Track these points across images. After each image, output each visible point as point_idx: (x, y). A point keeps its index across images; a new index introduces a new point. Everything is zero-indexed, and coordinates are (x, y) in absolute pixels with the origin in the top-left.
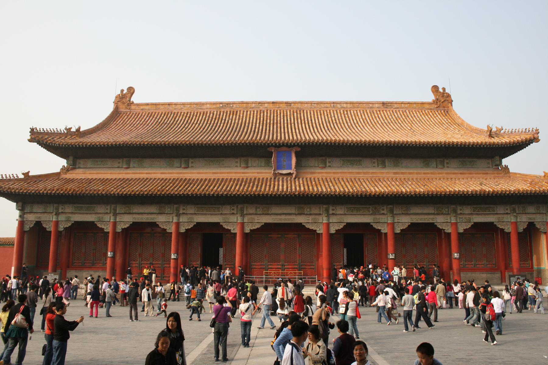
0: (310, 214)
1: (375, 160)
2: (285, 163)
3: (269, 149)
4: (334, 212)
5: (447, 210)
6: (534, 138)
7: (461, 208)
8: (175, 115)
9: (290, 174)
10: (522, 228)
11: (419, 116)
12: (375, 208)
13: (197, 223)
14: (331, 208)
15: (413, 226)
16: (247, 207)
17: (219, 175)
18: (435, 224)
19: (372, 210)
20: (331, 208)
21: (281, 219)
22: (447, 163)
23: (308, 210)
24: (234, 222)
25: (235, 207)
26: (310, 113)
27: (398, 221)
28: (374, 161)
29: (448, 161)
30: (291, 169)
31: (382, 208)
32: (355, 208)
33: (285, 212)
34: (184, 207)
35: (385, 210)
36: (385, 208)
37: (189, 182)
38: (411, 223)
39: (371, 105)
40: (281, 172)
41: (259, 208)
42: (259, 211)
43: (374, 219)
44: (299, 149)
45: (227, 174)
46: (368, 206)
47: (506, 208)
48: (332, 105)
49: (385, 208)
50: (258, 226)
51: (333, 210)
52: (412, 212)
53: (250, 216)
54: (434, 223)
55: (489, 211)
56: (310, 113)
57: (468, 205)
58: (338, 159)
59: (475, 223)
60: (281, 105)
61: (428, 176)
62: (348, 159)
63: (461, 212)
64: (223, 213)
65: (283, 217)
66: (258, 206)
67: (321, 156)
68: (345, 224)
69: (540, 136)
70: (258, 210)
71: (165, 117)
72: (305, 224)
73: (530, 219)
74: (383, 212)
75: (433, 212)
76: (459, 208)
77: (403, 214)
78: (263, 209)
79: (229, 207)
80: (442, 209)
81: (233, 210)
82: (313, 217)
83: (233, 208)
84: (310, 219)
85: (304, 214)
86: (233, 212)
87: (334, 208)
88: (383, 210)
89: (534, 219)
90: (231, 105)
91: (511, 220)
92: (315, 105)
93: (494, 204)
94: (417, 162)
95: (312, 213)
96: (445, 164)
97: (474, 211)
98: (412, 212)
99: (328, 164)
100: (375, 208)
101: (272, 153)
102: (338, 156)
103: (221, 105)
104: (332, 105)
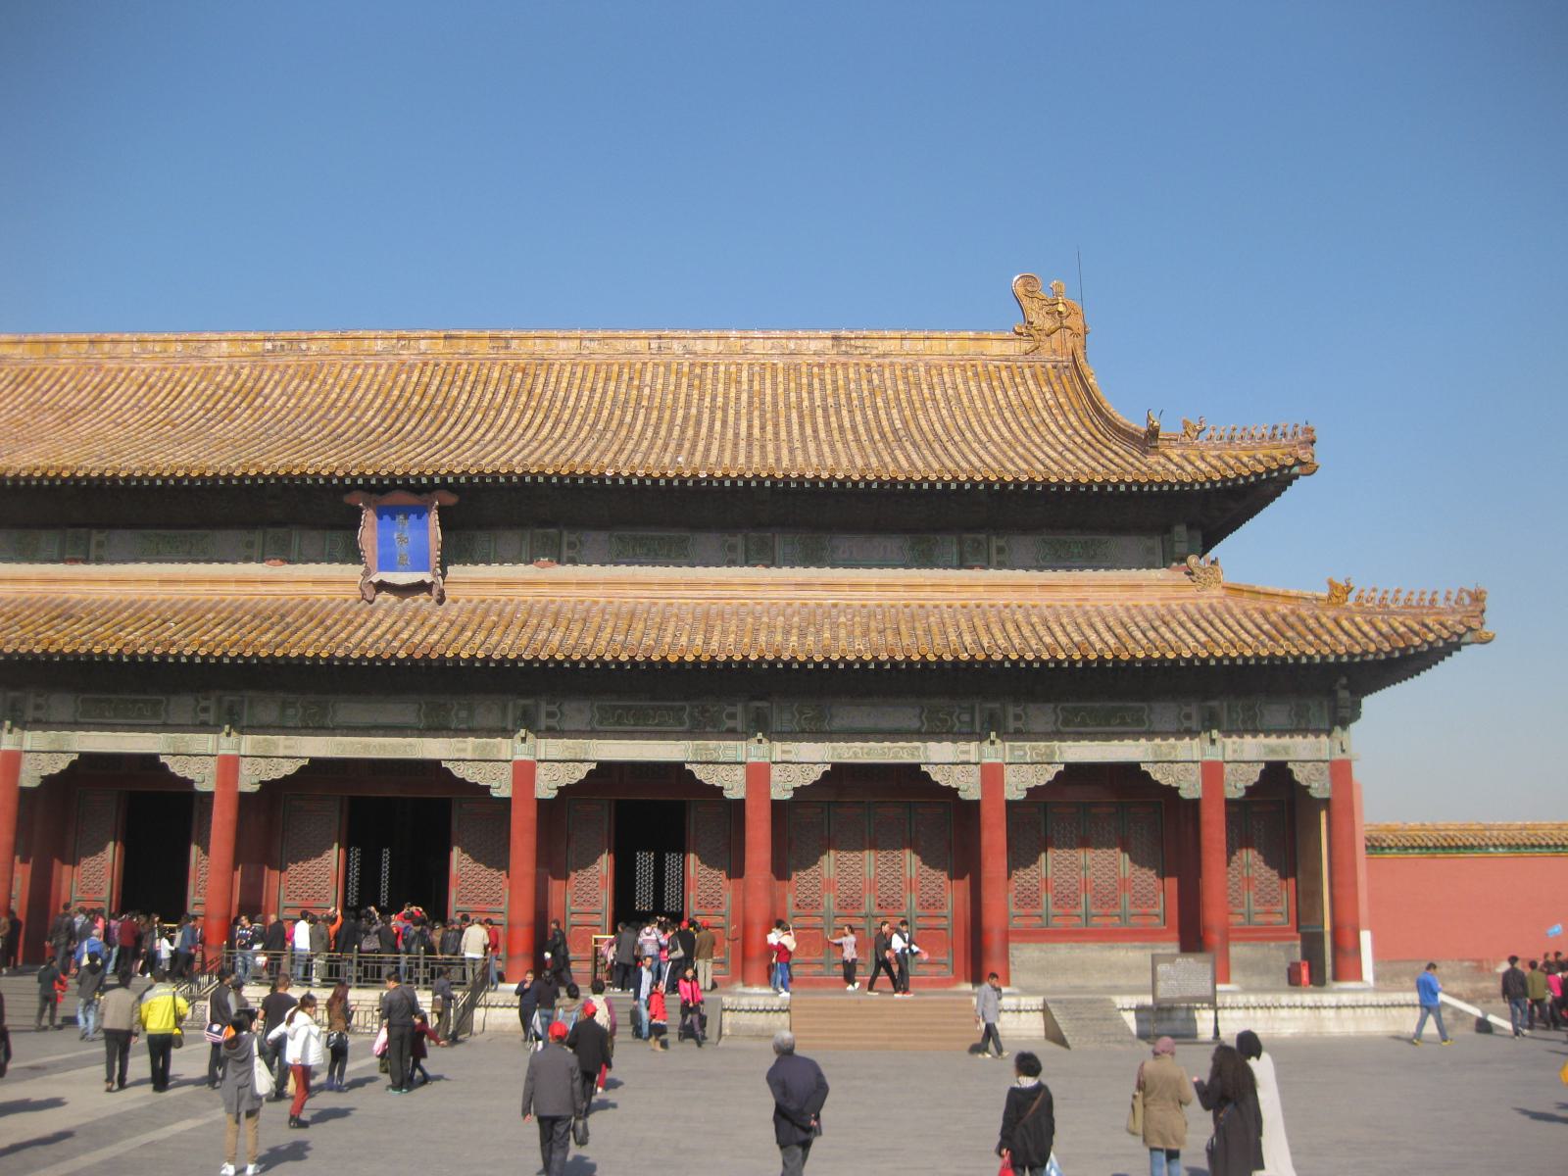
1: (739, 540)
2: (402, 549)
3: (347, 499)
4: (552, 722)
5: (966, 718)
6: (1299, 462)
7: (1018, 710)
8: (107, 380)
9: (422, 587)
10: (1241, 785)
11: (959, 381)
12: (704, 711)
13: (82, 755)
14: (544, 707)
15: (839, 774)
17: (181, 587)
18: (924, 768)
19: (691, 715)
20: (544, 707)
21: (367, 746)
22: (1000, 550)
23: (463, 714)
24: (208, 756)
25: (211, 703)
26: (573, 373)
27: (786, 758)
28: (732, 540)
29: (1002, 543)
30: (427, 570)
31: (730, 709)
32: (630, 708)
33: (383, 720)
34: (40, 701)
35: (739, 716)
36: (739, 709)
37: (65, 613)
38: (834, 765)
39: (792, 345)
40: (390, 577)
43: (697, 749)
44: (451, 500)
45: (207, 587)
46: (678, 704)
47: (1187, 710)
48: (654, 344)
49: (739, 709)
50: (289, 768)
51: (551, 715)
52: (837, 724)
54: (917, 766)
55: (1123, 723)
56: (573, 373)
57: (1048, 700)
58: (602, 536)
59: (1068, 765)
60: (476, 346)
61: (922, 595)
62: (640, 534)
63: (1019, 725)
64: (170, 722)
67: (544, 523)
68: (593, 766)
69: (1320, 454)
70: (290, 712)
71: (71, 385)
72: (449, 765)
73: (1272, 750)
74: (730, 724)
75: (915, 724)
76: (1011, 710)
77: (803, 731)
79: (188, 700)
80: (950, 714)
81: (205, 710)
83: (204, 704)
84: (469, 746)
86: (203, 717)
87: (553, 708)
88: (732, 716)
89: (1286, 749)
90: (304, 346)
91: (514, 753)
92: (594, 345)
93: (1143, 700)
94: (893, 544)
95: (475, 724)
96: (993, 551)
97: (1066, 723)
98: (837, 724)
99: (566, 553)
100: (704, 711)
101: (359, 512)
102: (599, 526)
103: (269, 346)
104: (654, 344)
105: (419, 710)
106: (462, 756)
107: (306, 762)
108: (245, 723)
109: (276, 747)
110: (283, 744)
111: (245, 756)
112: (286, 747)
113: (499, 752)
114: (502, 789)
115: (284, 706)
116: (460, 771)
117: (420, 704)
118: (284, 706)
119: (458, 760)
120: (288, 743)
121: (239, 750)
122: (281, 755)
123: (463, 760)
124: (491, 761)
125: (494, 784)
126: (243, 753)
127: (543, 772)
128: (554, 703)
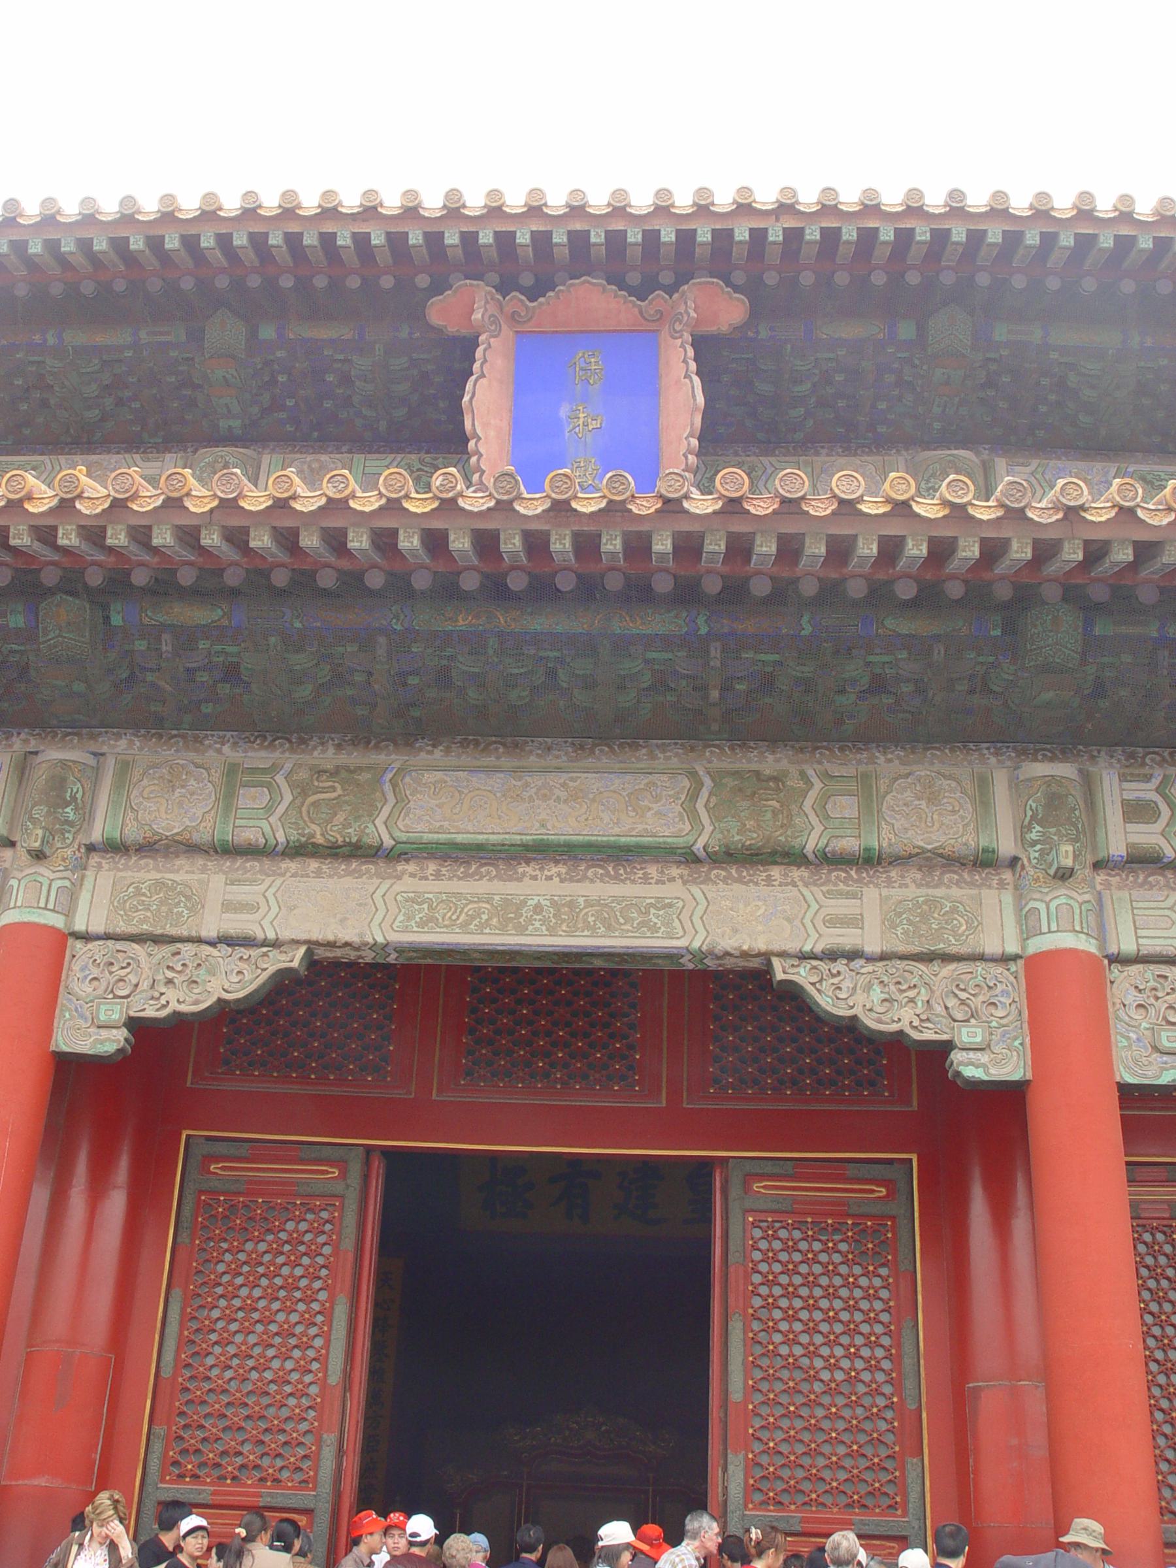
0: (870, 861)
16: (124, 768)
21: (509, 911)
23: (845, 807)
33: (565, 823)
41: (262, 777)
42: (262, 817)
44: (731, 312)
50: (233, 980)
53: (144, 873)
65: (540, 887)
66: (259, 757)
70: (251, 799)
72: (802, 975)
78: (302, 790)
82: (908, 888)
84: (869, 914)
85: (792, 857)
95: (882, 838)
105: (694, 796)
106: (847, 939)
107: (295, 959)
108: (96, 836)
109: (196, 906)
110: (222, 899)
111: (86, 937)
112: (228, 907)
113: (974, 925)
114: (989, 1055)
115: (233, 780)
116: (839, 995)
117: (693, 775)
118: (233, 780)
119: (831, 956)
120: (242, 893)
121: (69, 914)
122: (210, 931)
123: (853, 955)
124: (947, 958)
125: (969, 1035)
126: (80, 926)
127: (1132, 998)
128: (1148, 778)
